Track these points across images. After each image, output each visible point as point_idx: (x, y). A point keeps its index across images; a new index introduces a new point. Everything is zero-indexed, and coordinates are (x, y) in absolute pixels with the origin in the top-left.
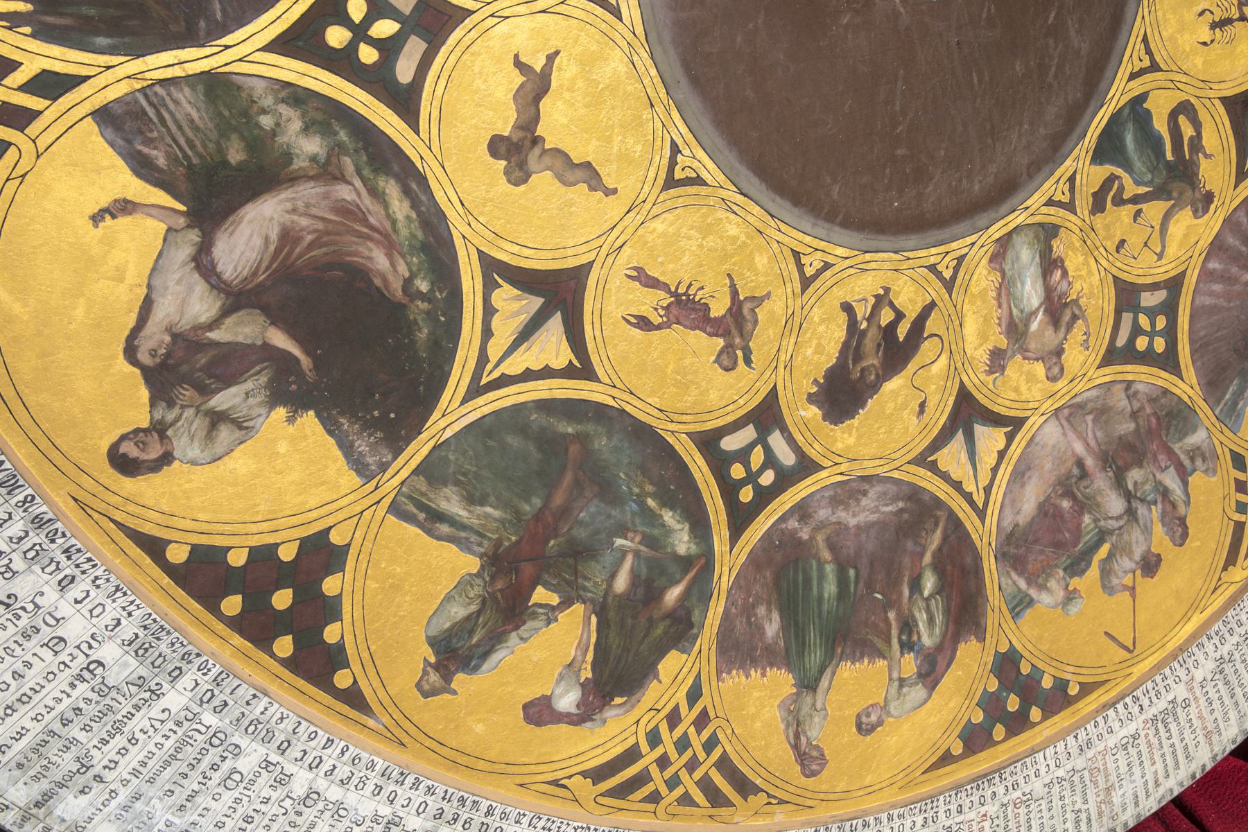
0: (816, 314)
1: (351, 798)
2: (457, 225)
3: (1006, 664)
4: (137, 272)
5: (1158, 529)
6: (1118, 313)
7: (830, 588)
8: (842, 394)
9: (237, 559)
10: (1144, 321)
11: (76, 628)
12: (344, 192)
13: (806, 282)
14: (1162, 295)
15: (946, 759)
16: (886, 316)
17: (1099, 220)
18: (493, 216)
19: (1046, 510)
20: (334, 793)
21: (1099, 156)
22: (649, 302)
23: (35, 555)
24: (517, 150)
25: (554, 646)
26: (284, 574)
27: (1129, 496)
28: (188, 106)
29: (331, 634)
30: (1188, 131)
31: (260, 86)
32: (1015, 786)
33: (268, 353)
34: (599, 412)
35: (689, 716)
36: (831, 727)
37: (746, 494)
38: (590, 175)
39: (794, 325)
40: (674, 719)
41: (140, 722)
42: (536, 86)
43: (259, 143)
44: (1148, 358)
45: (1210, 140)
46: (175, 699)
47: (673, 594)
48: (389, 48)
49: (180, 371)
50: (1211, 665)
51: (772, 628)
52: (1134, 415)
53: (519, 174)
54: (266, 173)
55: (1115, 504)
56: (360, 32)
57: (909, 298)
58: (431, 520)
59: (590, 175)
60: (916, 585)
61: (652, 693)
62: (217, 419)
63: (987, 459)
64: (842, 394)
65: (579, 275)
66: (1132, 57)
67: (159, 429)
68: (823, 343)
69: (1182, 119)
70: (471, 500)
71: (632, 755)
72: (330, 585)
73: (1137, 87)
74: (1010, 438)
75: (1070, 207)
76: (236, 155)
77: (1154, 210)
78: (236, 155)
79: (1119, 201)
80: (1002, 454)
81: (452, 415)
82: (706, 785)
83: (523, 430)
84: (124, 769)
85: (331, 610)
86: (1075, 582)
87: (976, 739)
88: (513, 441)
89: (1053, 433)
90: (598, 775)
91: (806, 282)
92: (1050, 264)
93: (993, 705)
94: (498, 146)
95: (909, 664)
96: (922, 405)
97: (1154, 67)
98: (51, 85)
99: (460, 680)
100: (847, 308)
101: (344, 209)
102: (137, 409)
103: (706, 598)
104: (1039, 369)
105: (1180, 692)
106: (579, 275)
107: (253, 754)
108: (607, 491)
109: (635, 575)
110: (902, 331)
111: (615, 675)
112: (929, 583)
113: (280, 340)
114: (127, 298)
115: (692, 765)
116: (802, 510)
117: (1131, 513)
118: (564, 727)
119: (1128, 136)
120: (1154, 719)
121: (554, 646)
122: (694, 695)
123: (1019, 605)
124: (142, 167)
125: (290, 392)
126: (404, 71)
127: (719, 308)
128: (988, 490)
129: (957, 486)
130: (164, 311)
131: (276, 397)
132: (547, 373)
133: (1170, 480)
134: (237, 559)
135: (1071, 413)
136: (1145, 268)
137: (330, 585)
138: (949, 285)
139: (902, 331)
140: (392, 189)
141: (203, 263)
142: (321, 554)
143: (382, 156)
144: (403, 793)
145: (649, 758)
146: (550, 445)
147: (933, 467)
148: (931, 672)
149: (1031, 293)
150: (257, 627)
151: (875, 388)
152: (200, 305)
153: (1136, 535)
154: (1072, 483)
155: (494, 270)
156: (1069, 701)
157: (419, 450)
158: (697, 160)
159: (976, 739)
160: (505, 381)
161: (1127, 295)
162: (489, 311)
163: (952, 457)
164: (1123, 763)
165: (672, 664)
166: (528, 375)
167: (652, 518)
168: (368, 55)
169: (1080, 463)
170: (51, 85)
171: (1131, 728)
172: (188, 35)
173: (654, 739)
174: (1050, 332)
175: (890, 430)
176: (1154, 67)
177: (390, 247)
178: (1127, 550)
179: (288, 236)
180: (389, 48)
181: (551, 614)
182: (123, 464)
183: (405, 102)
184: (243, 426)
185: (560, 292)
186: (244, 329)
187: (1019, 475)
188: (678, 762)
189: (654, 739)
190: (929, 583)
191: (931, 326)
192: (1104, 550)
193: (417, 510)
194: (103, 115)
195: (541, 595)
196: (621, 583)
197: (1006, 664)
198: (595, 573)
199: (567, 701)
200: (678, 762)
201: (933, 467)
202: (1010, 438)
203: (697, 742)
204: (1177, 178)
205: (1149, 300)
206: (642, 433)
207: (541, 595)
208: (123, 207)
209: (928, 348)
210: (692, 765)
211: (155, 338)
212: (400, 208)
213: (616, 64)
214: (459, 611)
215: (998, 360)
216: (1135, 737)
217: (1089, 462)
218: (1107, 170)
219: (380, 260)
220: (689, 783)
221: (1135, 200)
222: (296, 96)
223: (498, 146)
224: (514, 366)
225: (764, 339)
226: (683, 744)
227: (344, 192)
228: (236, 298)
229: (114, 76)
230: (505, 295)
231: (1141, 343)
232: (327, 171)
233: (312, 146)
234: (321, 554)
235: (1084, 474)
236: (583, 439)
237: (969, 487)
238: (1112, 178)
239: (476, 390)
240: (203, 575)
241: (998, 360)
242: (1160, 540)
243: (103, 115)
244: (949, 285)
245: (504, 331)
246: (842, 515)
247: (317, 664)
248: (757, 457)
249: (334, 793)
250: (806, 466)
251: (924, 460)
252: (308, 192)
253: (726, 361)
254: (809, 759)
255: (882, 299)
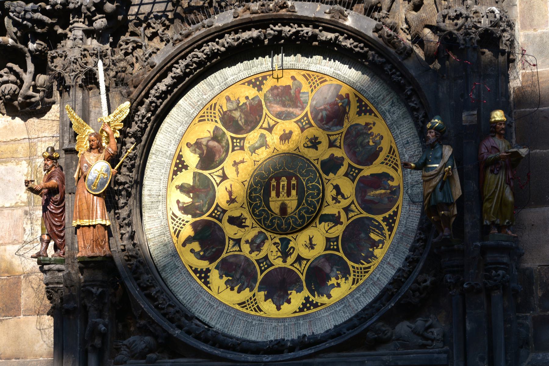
0: (239, 211)
1: (162, 184)
2: (225, 162)
3: (208, 270)
4: (205, 136)
5: (238, 286)
6: (263, 258)
7: (207, 234)
8: (232, 221)
9: (182, 159)
10: (265, 263)
11: (170, 148)
12: (222, 150)
13: (241, 207)
14: (270, 264)
15: (191, 267)
16: (244, 221)
17: (273, 245)
18: (228, 165)
19: (232, 263)
20: (162, 182)
21: (280, 239)
22: (229, 188)
23: (176, 141)
24: (236, 164)
25: (186, 200)
26: (183, 165)
27: (240, 278)
28: (221, 132)
29: (179, 173)
30: (291, 251)
31: (226, 138)
32: (191, 282)
33: (203, 151)
34: (214, 190)
35: (184, 223)
36: (189, 246)
37: (214, 214)
38: (238, 173)
39: (236, 208)
40: (183, 221)
41: (163, 158)
42: (242, 162)
43: (222, 139)
44: (260, 267)
45: (293, 256)
46: (167, 160)
47: (198, 212)
48: (237, 146)
49: (198, 144)
50: (221, 309)
51: (199, 228)
52: (252, 271)
53: (233, 165)
54: (219, 142)
55: (238, 276)
56: (236, 142)
57: (248, 222)
58: (194, 177)
59: (238, 173)
60: (213, 248)
61: (185, 216)
62: (195, 150)
63: (234, 249)
64: (232, 221)
65: (227, 178)
66: (294, 236)
67: (192, 145)
68: (236, 214)
69: (292, 249)
70: (198, 180)
71: (177, 217)
72: (183, 170)
73: (291, 239)
74: (239, 251)
75: (272, 240)
76: (219, 138)
77: (279, 254)
78: (219, 138)
79: (277, 247)
80: (236, 251)
81: (206, 173)
82: (176, 229)
83: (208, 182)
84: (159, 159)
85: (181, 171)
86: (224, 276)
87: (196, 271)
88: (207, 181)
89: (242, 258)
90: (173, 214)
91: (241, 207)
92: (263, 242)
93: (202, 271)
94: (235, 161)
95: (202, 253)
96: (236, 234)
97: (295, 239)
98: (216, 121)
99: (178, 190)
100: (242, 214)
101: (220, 150)
102: (192, 143)
103: (199, 216)
104: (250, 249)
105: (215, 307)
106: (227, 178)
107: (163, 171)
108: (206, 196)
109: (198, 205)
110: (243, 224)
111: (185, 209)
112: (214, 250)
113: (205, 152)
114: (202, 136)
115: (178, 226)
116: (215, 223)
117: (238, 279)
118: (177, 206)
119: (285, 242)
120: (209, 303)
121: (186, 200)
122: (187, 222)
123: (217, 268)
124: (214, 132)
125: (200, 156)
126: (236, 148)
127: (233, 197)
128: (230, 252)
129: (229, 246)
130: (203, 140)
131: (200, 154)
132: (215, 181)
133: (246, 284)
134: (182, 159)
135: (247, 259)
136: (271, 258)
137: (183, 170)
138: (252, 227)
139: (243, 224)
140: (225, 154)
141: (208, 141)
142: (186, 167)
143: (227, 151)
144: (164, 190)
145: (177, 220)
146: (208, 186)
147: (229, 241)
148: (202, 258)
149: (258, 241)
150: (177, 165)
151: (234, 225)
152: (205, 143)
153: (235, 283)
154: (238, 265)
155: (223, 168)
156: (207, 286)
157: (201, 171)
158: (246, 184)
159: (196, 271)
160: (212, 176)
161: (266, 258)
162: (218, 171)
163: (231, 242)
164: (201, 302)
165: (190, 216)
166: (214, 179)
167: (206, 204)
168: (235, 144)
169: (241, 265)
170: (216, 121)
171: (207, 299)
172: (227, 129)
173: (180, 219)
174: (255, 248)
175: (230, 230)
176: (295, 239)
177: (219, 157)
178: (233, 283)
179: (215, 147)
180: (237, 146)
181: (190, 197)
182: (187, 144)
183: (233, 150)
184: (195, 153)
185: (224, 177)
186: (204, 148)
187: (235, 256)
188: (178, 224)
189: (180, 219)
190: (214, 250)
191: (246, 228)
192: (230, 278)
193: (195, 174)
194: (216, 126)
195: (191, 194)
196: (197, 204)
197: (208, 270)
198: (196, 200)
199: (181, 205)
200: (178, 224)
201: (229, 241)
202: (239, 251)
203: (181, 225)
204: (285, 255)
205: (268, 262)
206: (214, 196)
207: (191, 194)
208: (210, 132)
209: (243, 230)
210: (178, 226)
211: (200, 141)
212: (223, 156)
213: (250, 169)
214: (186, 186)
215: (247, 242)
216: (206, 301)
217: (242, 267)
218: (279, 242)
219: (217, 157)
220: (176, 227)
221: (278, 249)
222: (227, 140)
223: (235, 161)
224: (215, 177)
225: (232, 205)
226: (180, 224)
227: (222, 150)
228: (207, 146)
229: (220, 125)
230: (221, 171)
231: (262, 265)
232: (223, 147)
233: (224, 144)
234: (186, 167)
235: (239, 267)
236: (211, 189)
237: (229, 248)
238: (278, 243)
239: (210, 174)
240: (180, 157)
241: (247, 242)
242: (236, 288)
243: (216, 126)
244: (252, 227)
245: (217, 173)
246: (217, 230)
247: (175, 173)
248: (219, 213)
249: (162, 182)
250: (220, 221)
251: (229, 238)
252: (220, 146)
253: (228, 202)
254: (184, 245)
255: (245, 219)
